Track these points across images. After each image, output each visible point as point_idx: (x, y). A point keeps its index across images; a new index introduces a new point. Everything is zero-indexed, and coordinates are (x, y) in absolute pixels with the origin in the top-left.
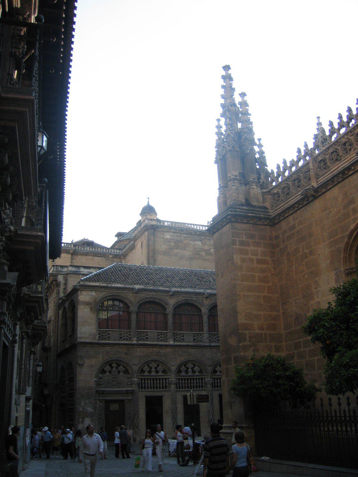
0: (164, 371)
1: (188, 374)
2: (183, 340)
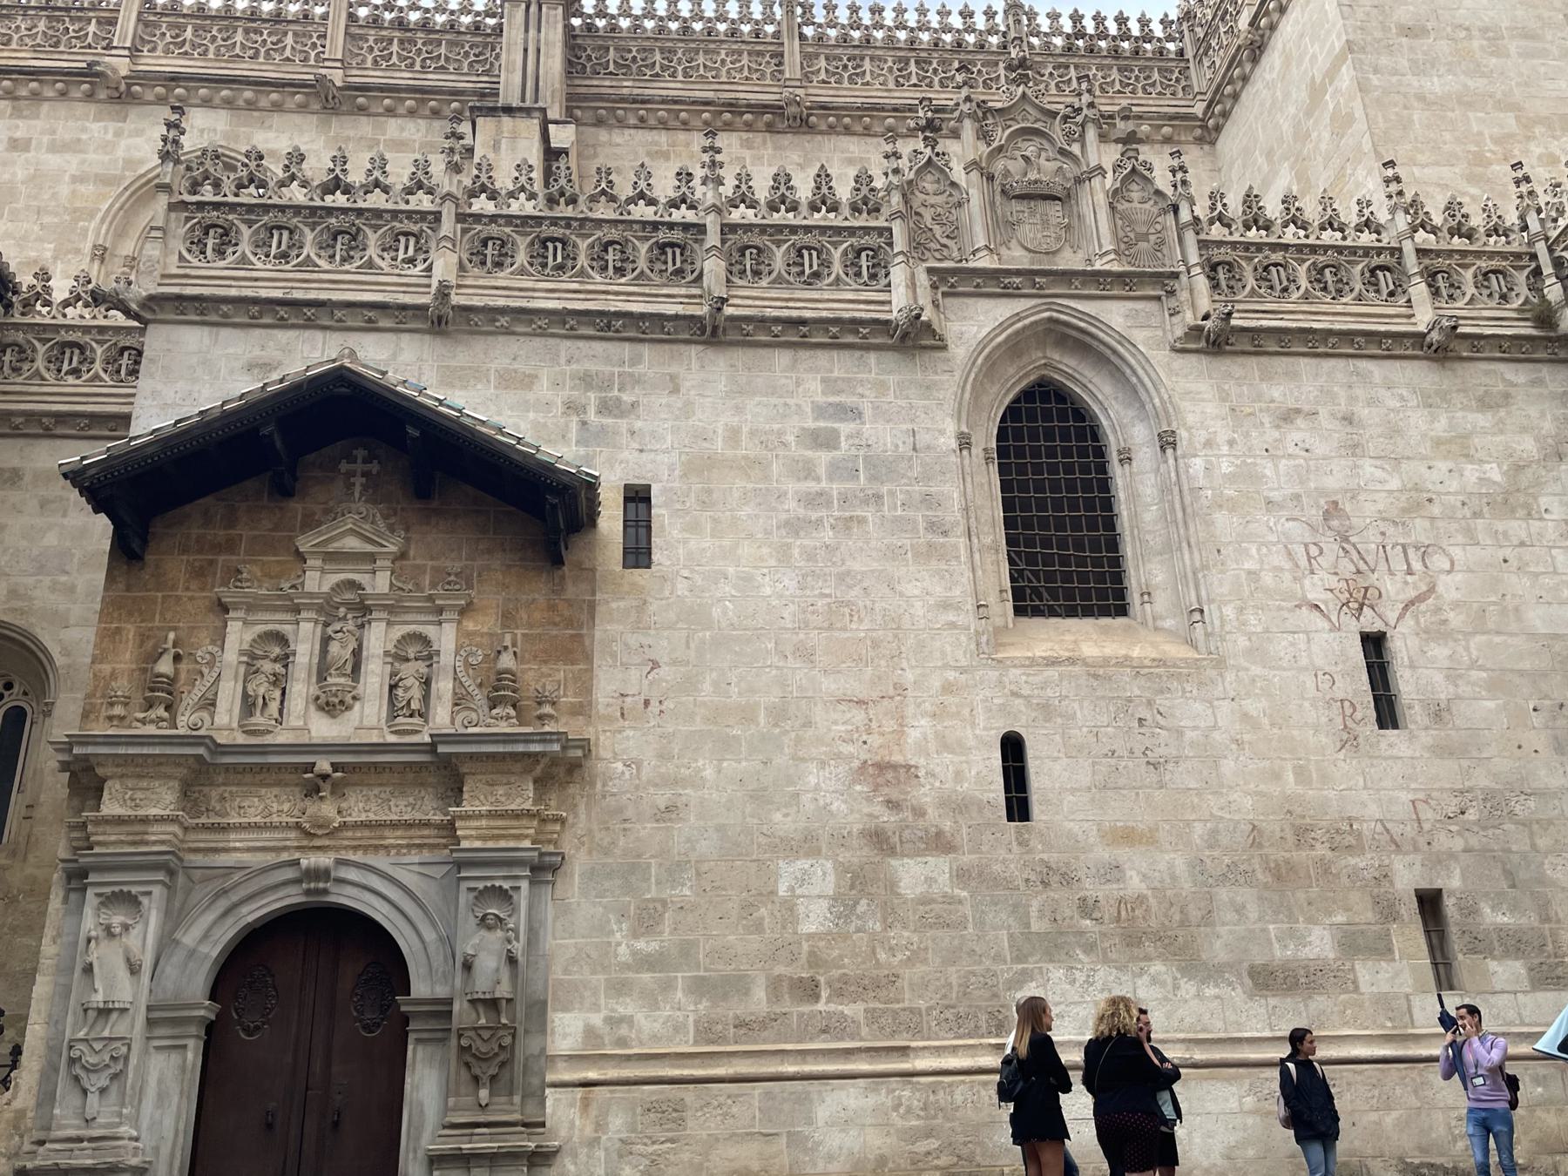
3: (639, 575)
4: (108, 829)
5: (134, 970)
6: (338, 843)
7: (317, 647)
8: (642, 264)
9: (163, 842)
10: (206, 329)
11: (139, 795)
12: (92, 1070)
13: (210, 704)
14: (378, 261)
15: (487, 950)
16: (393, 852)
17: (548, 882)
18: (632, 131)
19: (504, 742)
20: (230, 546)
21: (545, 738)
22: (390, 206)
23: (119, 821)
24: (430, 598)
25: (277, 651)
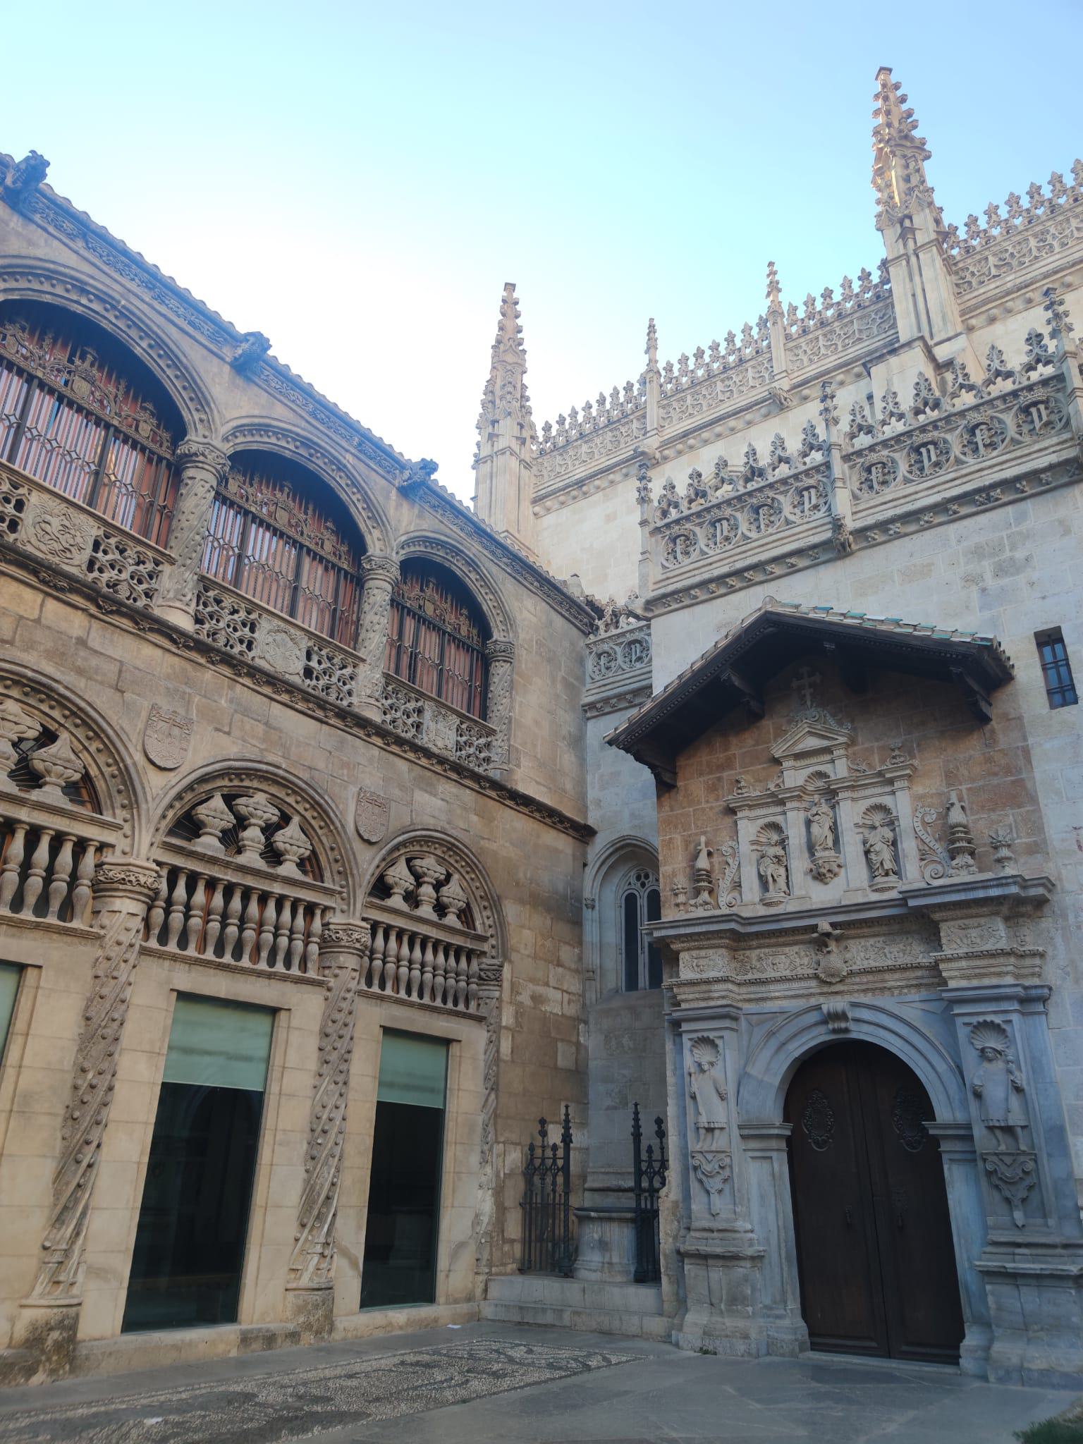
0: (82, 789)
1: (241, 859)
2: (249, 647)
3: (1068, 712)
4: (686, 989)
5: (722, 1098)
6: (851, 987)
7: (803, 830)
8: (1012, 431)
9: (723, 997)
10: (686, 611)
11: (702, 962)
13: (737, 885)
14: (792, 518)
15: (992, 1079)
16: (896, 992)
17: (1039, 1013)
18: (1024, 314)
19: (964, 890)
20: (728, 764)
21: (1000, 882)
22: (793, 472)
23: (692, 983)
24: (880, 774)
25: (775, 837)
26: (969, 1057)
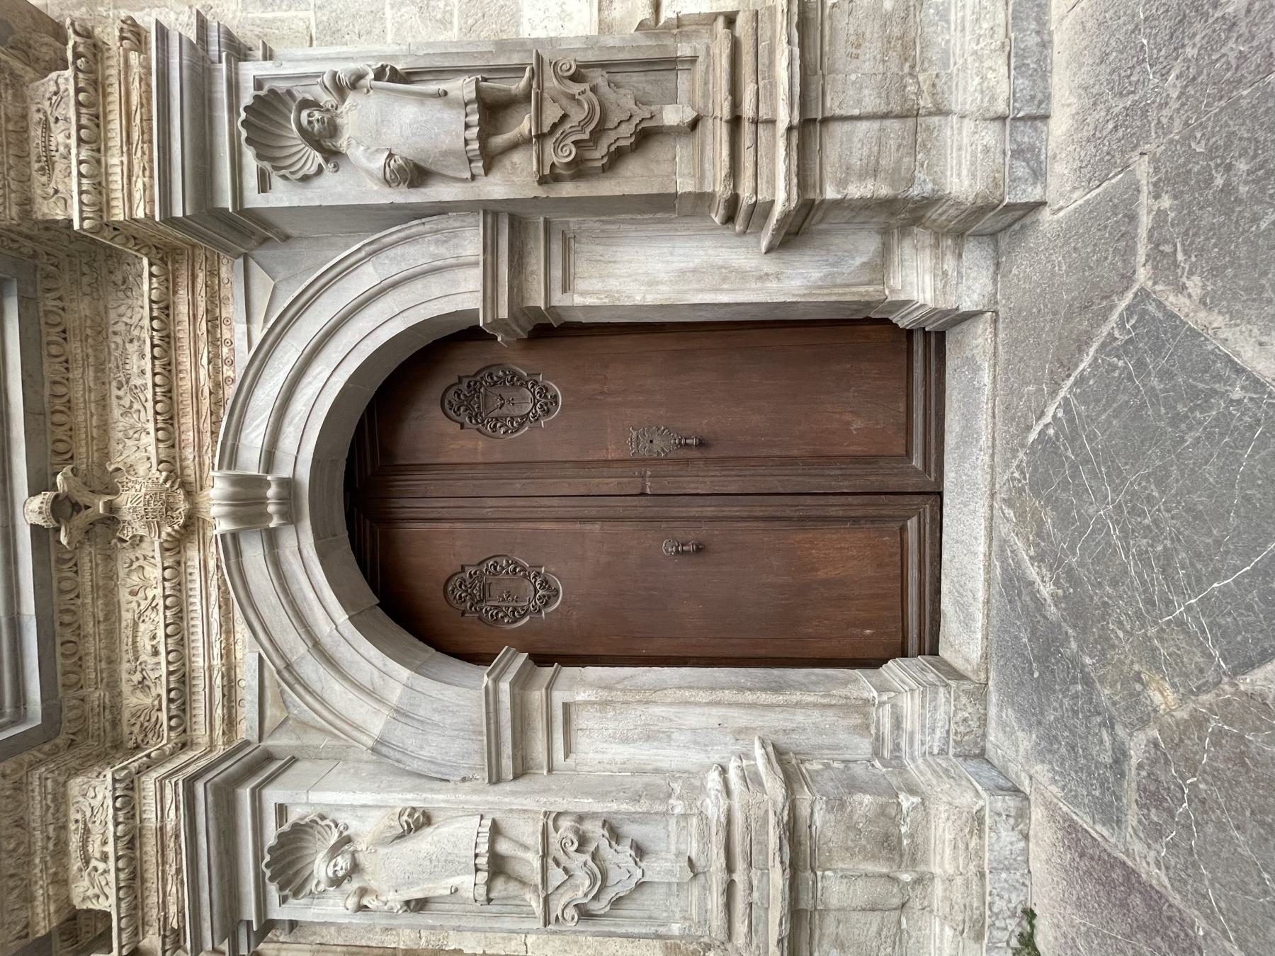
5: (421, 821)
12: (601, 879)
26: (335, 189)
